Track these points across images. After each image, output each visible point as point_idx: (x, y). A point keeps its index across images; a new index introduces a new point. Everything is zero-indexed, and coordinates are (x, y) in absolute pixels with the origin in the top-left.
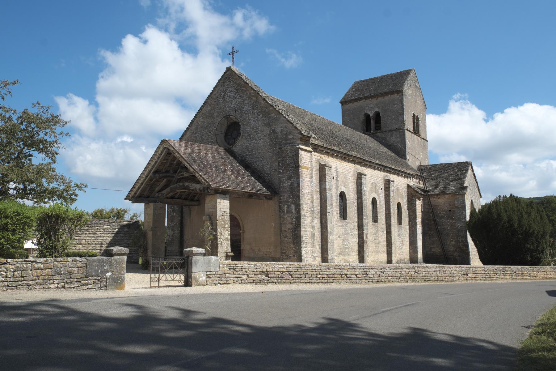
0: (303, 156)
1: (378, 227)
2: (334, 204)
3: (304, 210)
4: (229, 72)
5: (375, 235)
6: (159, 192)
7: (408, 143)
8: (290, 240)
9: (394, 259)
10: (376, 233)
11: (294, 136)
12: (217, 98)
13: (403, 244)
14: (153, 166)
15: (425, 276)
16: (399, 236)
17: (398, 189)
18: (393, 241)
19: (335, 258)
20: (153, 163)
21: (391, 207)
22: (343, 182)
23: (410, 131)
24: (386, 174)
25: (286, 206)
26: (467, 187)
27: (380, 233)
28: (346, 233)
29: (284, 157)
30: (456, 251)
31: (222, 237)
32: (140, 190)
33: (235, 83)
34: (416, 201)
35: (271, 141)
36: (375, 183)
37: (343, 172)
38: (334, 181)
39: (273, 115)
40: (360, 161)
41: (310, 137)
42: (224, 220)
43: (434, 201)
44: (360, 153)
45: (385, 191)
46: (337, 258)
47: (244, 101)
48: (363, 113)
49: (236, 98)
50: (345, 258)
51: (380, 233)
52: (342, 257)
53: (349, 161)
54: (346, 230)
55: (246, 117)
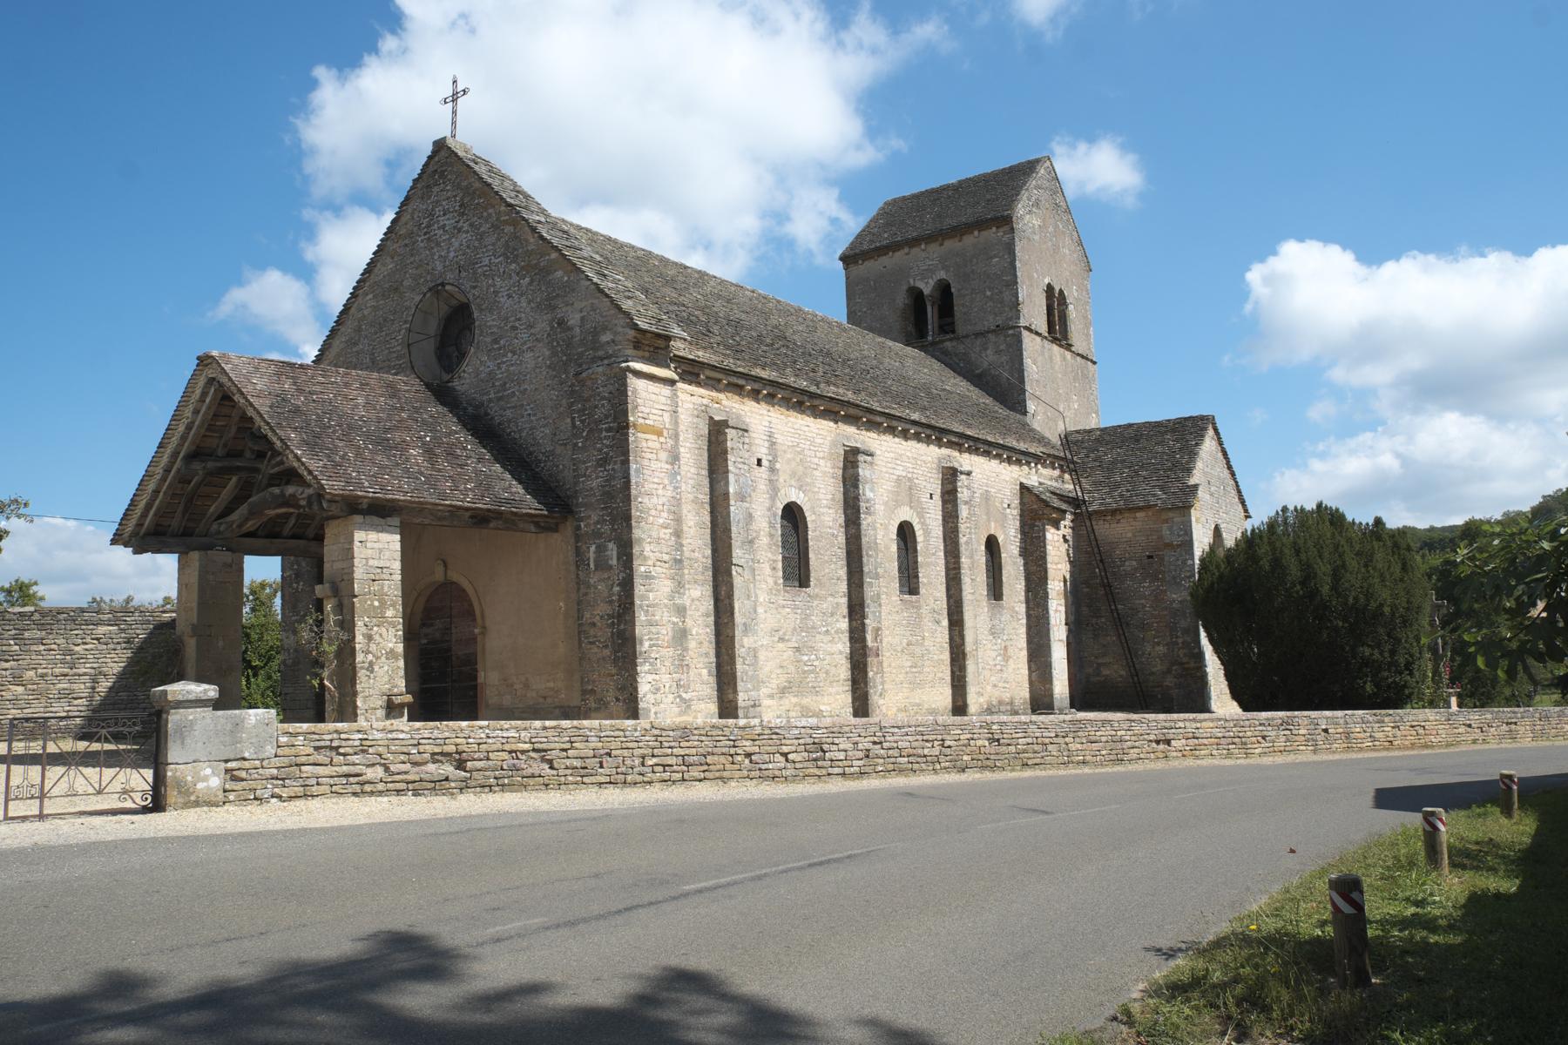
0: (643, 394)
1: (919, 608)
2: (764, 540)
3: (645, 558)
4: (443, 153)
5: (907, 635)
6: (219, 517)
7: (1031, 367)
8: (607, 652)
9: (974, 701)
10: (915, 624)
11: (616, 333)
12: (410, 234)
13: (1006, 658)
14: (183, 438)
15: (1025, 751)
16: (993, 632)
17: (987, 497)
18: (969, 647)
19: (766, 702)
20: (182, 428)
21: (963, 548)
22: (793, 474)
23: (1037, 333)
24: (945, 451)
25: (593, 548)
26: (1196, 487)
27: (928, 624)
28: (806, 628)
29: (588, 400)
30: (1169, 671)
31: (373, 647)
32: (152, 513)
33: (458, 187)
34: (1044, 531)
35: (554, 354)
36: (910, 480)
37: (790, 450)
38: (763, 472)
39: (559, 274)
40: (852, 411)
41: (668, 338)
42: (381, 596)
43: (1104, 529)
44: (857, 392)
45: (944, 502)
46: (769, 702)
47: (481, 237)
48: (905, 287)
49: (459, 230)
50: (805, 701)
51: (928, 624)
52: (794, 700)
53: (816, 413)
54: (807, 617)
55: (489, 286)
